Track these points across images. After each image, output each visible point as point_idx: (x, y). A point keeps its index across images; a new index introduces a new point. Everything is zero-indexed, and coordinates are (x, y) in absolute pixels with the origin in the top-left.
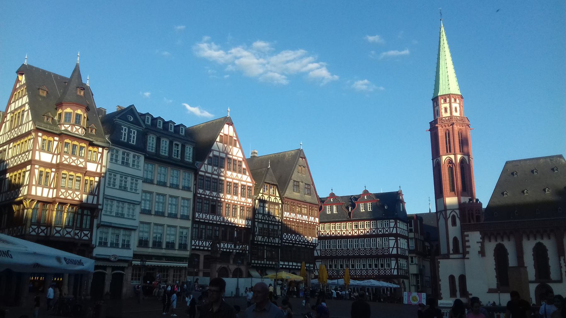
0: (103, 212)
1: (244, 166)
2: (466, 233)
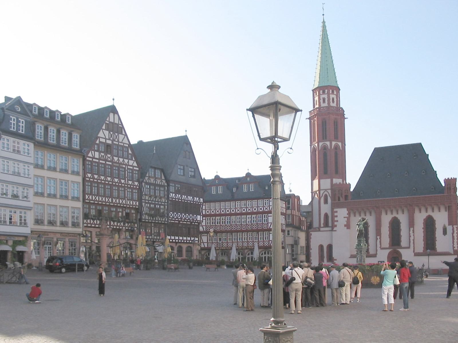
1: (130, 152)
2: (335, 210)
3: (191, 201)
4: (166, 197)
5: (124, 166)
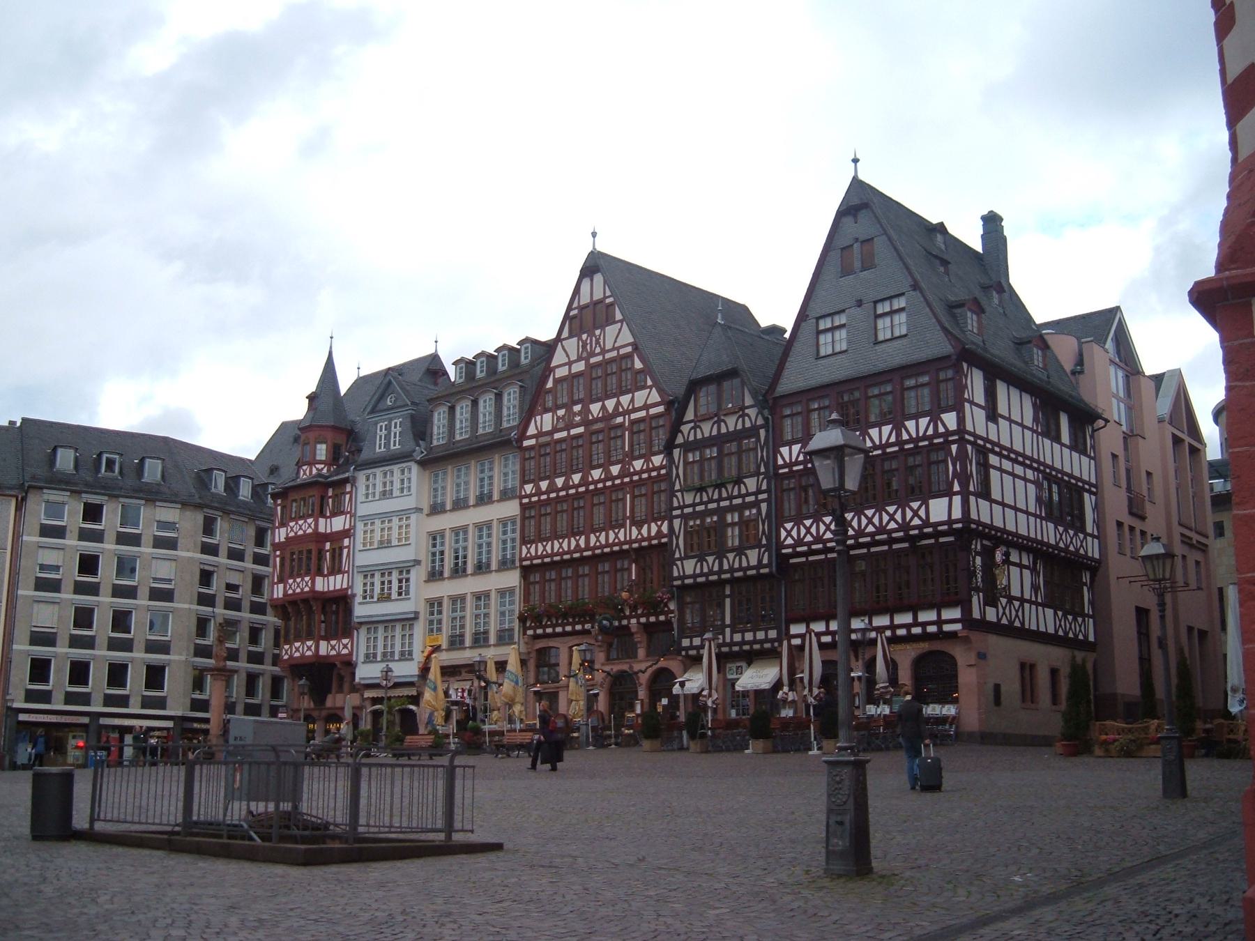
0: (358, 599)
3: (882, 447)
4: (763, 470)
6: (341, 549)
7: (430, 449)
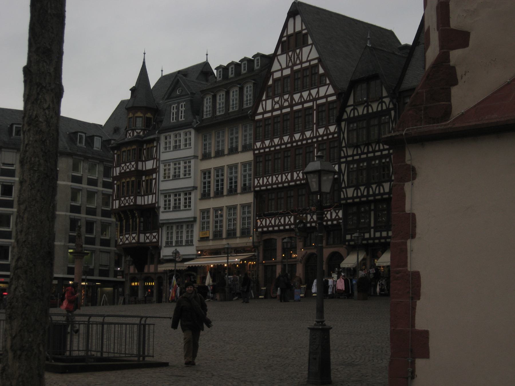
0: (162, 209)
5: (310, 104)
6: (151, 180)
7: (202, 121)
